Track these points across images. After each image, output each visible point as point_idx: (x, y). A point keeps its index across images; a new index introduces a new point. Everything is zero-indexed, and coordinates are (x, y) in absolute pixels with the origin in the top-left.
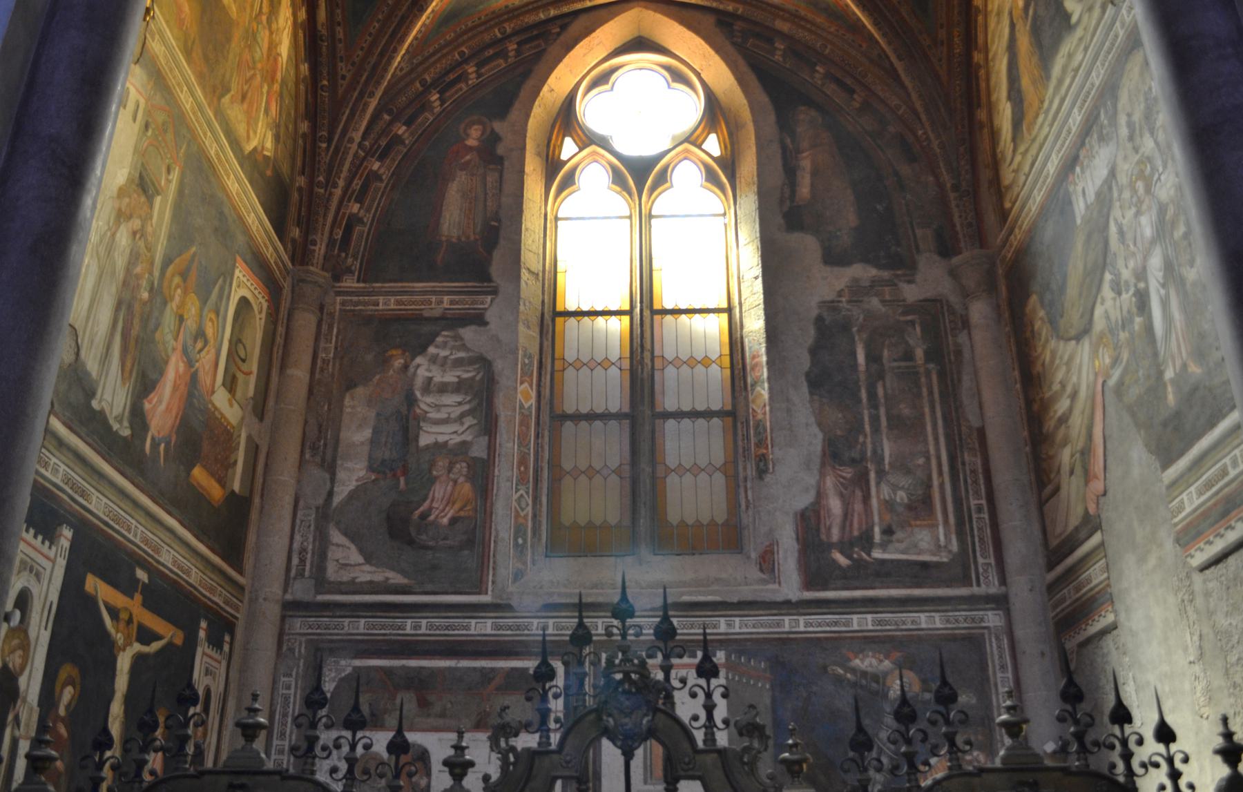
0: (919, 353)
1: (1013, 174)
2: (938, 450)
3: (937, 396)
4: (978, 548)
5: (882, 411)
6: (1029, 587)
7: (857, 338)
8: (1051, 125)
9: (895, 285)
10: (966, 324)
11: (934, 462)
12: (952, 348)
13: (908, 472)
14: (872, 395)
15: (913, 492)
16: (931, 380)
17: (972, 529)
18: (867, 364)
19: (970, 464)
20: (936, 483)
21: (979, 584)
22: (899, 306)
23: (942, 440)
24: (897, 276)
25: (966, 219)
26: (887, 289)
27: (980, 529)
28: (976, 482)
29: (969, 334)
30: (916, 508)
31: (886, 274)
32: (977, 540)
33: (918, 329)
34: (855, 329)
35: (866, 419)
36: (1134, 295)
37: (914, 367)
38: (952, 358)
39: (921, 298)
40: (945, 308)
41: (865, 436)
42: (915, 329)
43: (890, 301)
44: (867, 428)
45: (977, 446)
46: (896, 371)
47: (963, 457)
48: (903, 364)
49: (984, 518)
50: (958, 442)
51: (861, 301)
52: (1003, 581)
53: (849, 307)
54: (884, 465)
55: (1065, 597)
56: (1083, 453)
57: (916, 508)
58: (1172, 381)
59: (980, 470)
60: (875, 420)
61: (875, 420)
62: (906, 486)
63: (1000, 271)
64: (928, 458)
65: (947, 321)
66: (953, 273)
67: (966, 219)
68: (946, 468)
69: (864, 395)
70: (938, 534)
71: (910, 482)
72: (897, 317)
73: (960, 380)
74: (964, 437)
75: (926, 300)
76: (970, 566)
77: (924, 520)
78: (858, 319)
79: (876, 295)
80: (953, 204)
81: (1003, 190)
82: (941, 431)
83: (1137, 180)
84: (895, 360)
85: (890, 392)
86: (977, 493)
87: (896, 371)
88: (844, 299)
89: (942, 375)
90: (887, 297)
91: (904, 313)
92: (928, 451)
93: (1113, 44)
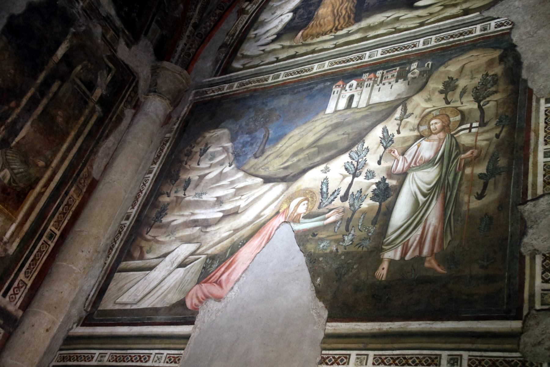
0: (99, 92)
1: (262, 52)
2: (58, 167)
3: (86, 131)
4: (27, 265)
5: (45, 101)
6: (49, 327)
7: (69, 37)
8: (336, 46)
9: (119, 36)
10: (137, 107)
11: (49, 173)
12: (118, 112)
13: (25, 162)
14: (47, 84)
15: (17, 181)
16: (91, 118)
17: (34, 247)
18: (61, 60)
19: (70, 198)
20: (38, 189)
21: (4, 295)
22: (110, 50)
23: (66, 163)
24: (124, 32)
25: (189, 49)
26: (112, 31)
27: (39, 251)
28: (64, 214)
29: (134, 115)
30: (8, 194)
31: (118, 23)
32: (32, 258)
33: (110, 77)
34: (73, 30)
35: (29, 94)
36: (377, 184)
37: (88, 98)
38: (114, 119)
39: (127, 62)
40: (134, 84)
41: (18, 105)
42: (108, 75)
43: (107, 41)
44: (24, 101)
45: (84, 190)
46: (75, 86)
47: (70, 188)
48: (83, 87)
49: (49, 245)
50: (74, 175)
51: (91, 19)
52: (26, 306)
53: (81, 12)
54: (13, 140)
55: (93, 358)
56: (212, 258)
57: (8, 194)
58: (392, 262)
59: (73, 209)
60: (34, 102)
61: (34, 102)
62: (16, 171)
63: (191, 98)
64: (47, 166)
65: (129, 93)
66: (155, 71)
67: (189, 49)
68: (53, 185)
69: (41, 77)
70: (8, 229)
71: (21, 170)
72: (104, 56)
73: (107, 136)
74: (81, 175)
75: (127, 66)
76: (11, 275)
77: (7, 208)
78: (80, 26)
79: (103, 27)
80: (188, 33)
81: (239, 55)
82: (71, 156)
83: (435, 117)
84: (80, 79)
85: (60, 94)
86: (59, 222)
87: (75, 86)
88: (81, 4)
89: (100, 122)
90: (108, 37)
91: (109, 58)
92: (51, 162)
93: (461, 34)
